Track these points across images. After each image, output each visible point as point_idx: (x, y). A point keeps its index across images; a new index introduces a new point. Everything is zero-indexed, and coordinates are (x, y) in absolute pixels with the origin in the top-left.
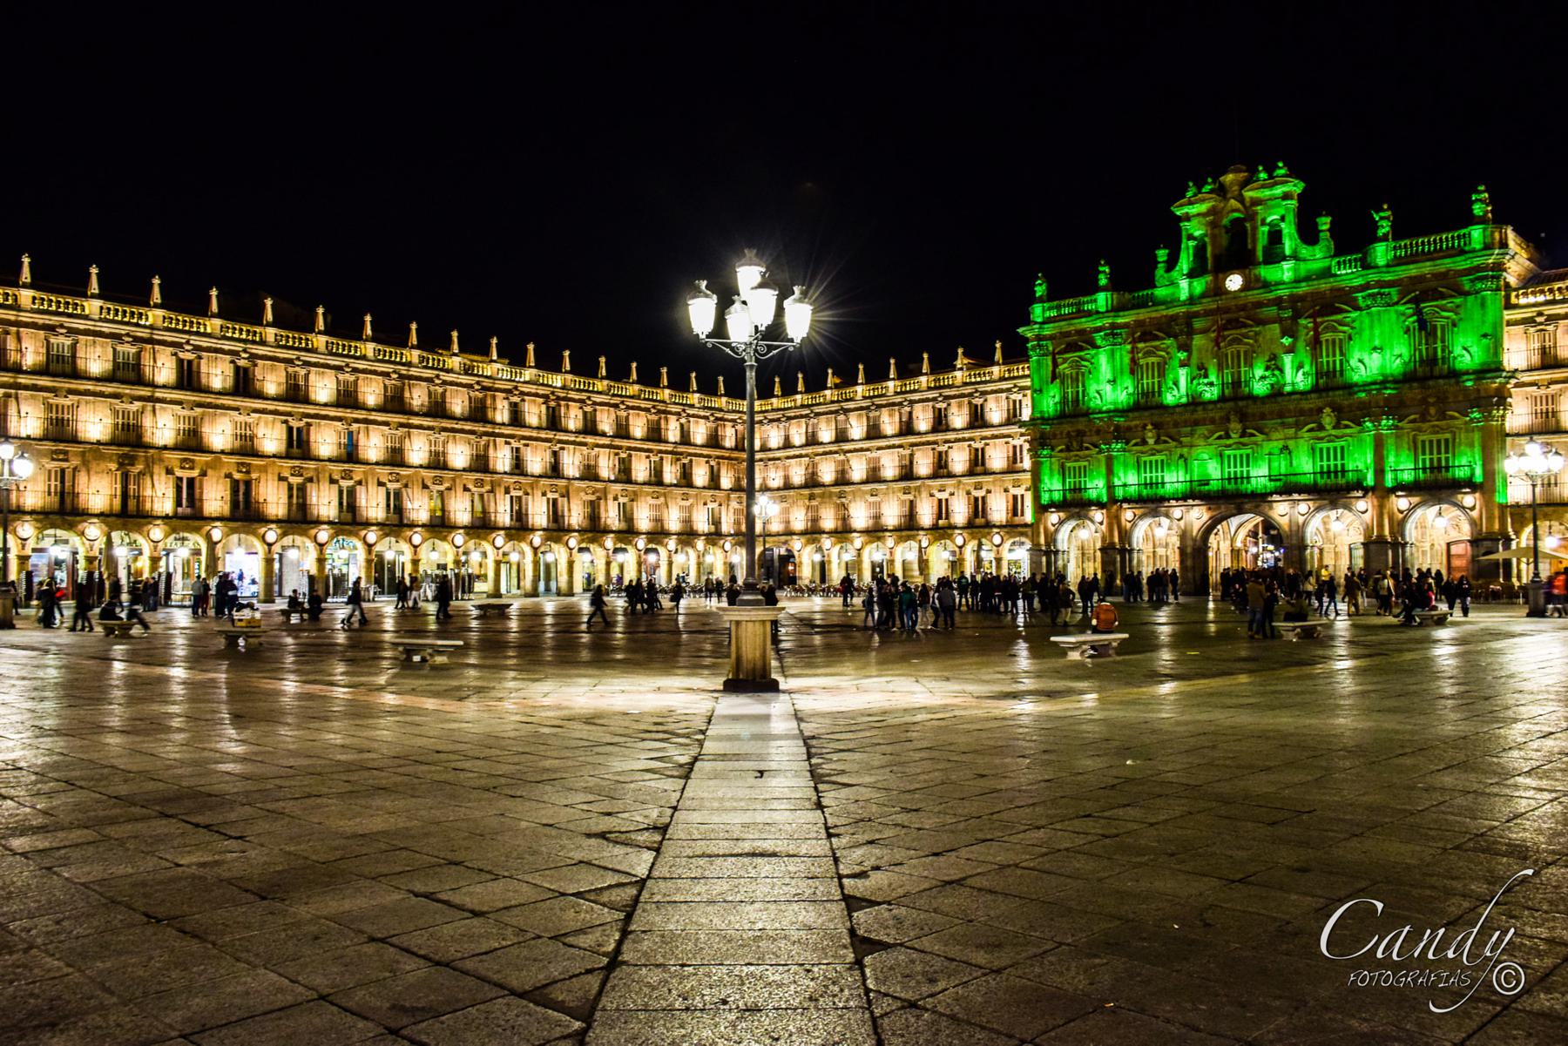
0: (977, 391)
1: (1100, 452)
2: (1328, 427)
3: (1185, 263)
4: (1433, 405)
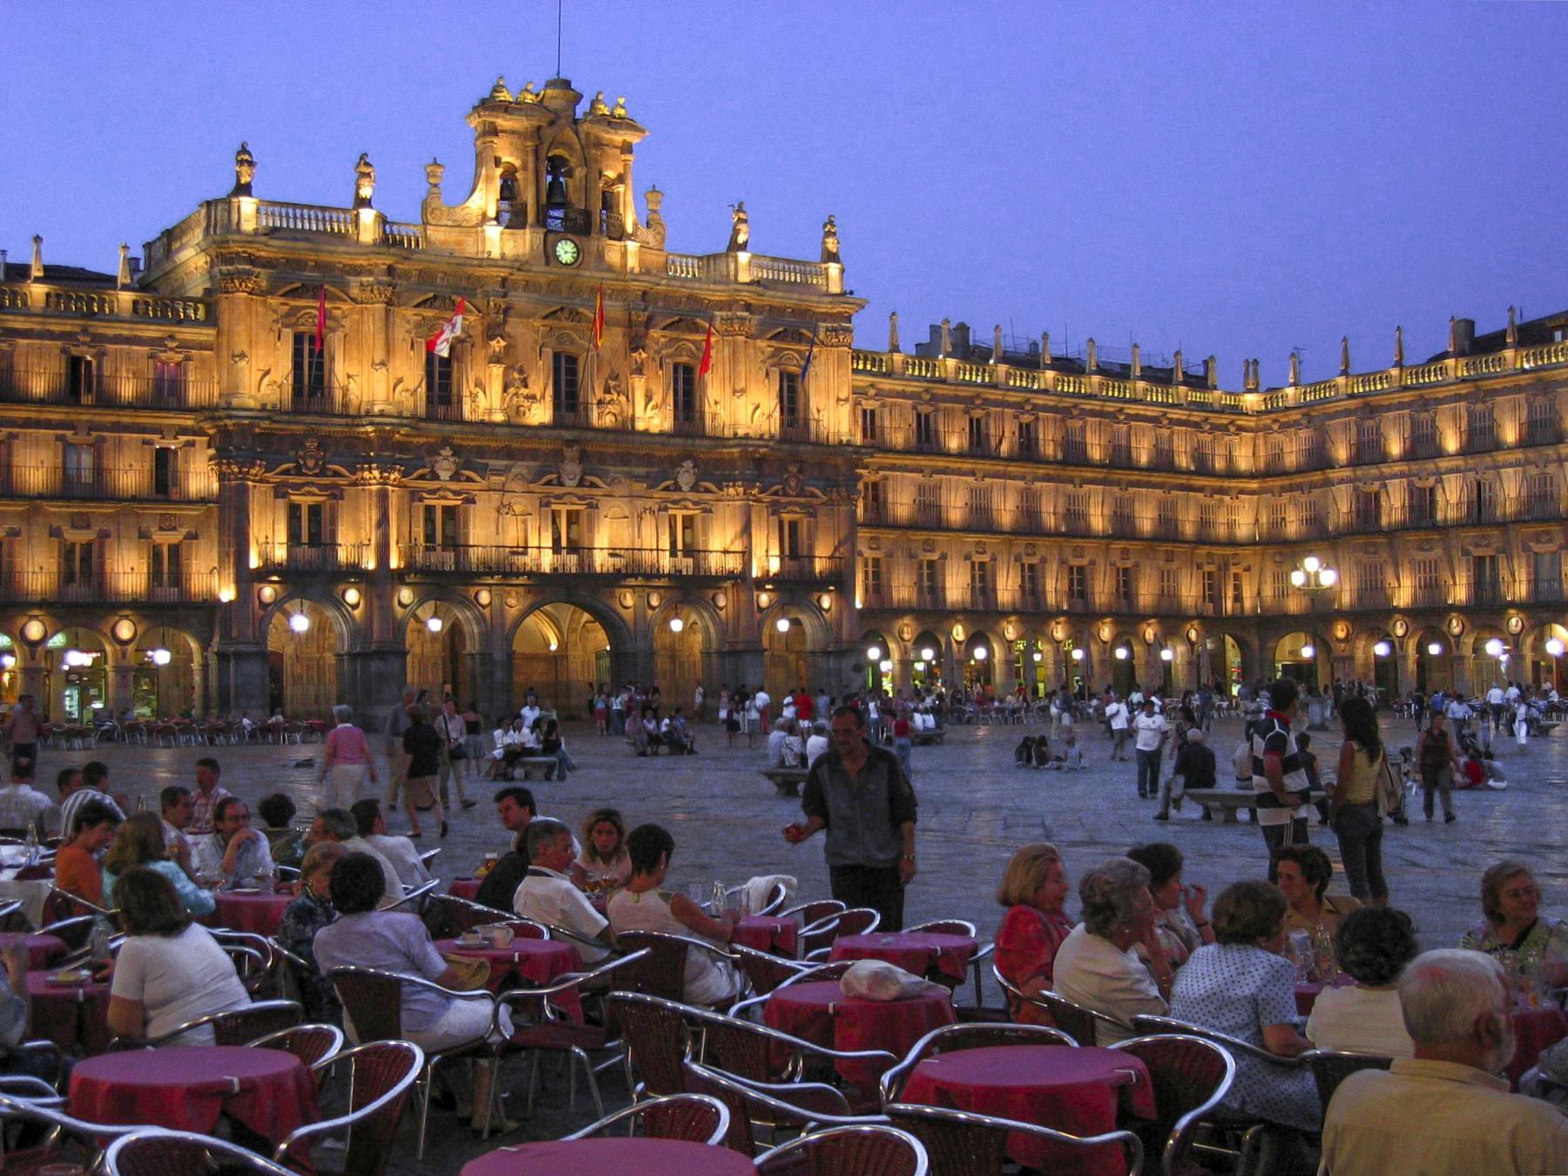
0: (85, 331)
1: (354, 484)
2: (685, 488)
4: (794, 476)
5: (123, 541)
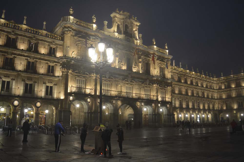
0: (34, 37)
1: (90, 77)
2: (147, 84)
3: (115, 28)
5: (39, 84)
